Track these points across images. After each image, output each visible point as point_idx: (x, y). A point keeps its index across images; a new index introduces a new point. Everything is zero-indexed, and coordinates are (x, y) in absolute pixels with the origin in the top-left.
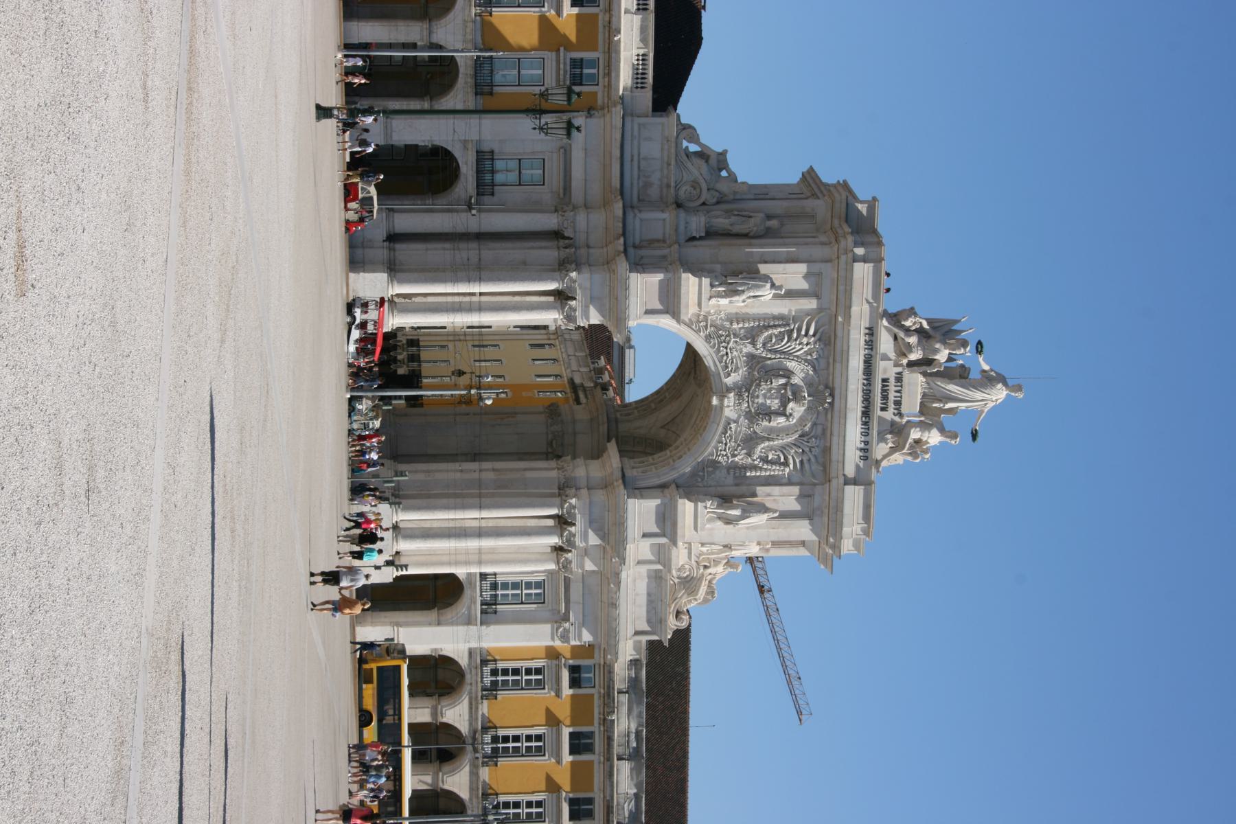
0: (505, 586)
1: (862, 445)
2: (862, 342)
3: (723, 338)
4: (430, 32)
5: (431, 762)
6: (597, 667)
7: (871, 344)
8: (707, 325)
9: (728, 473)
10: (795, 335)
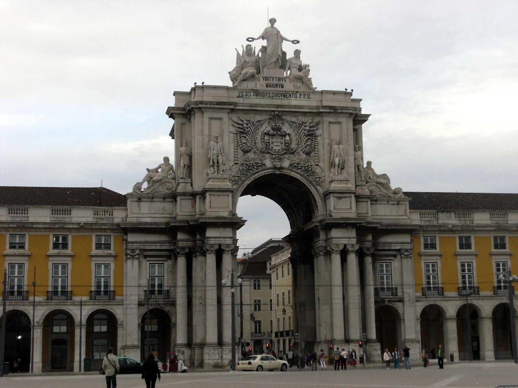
1: (302, 97)
2: (247, 97)
5: (478, 322)
6: (424, 235)
8: (237, 176)
9: (317, 165)
10: (242, 131)
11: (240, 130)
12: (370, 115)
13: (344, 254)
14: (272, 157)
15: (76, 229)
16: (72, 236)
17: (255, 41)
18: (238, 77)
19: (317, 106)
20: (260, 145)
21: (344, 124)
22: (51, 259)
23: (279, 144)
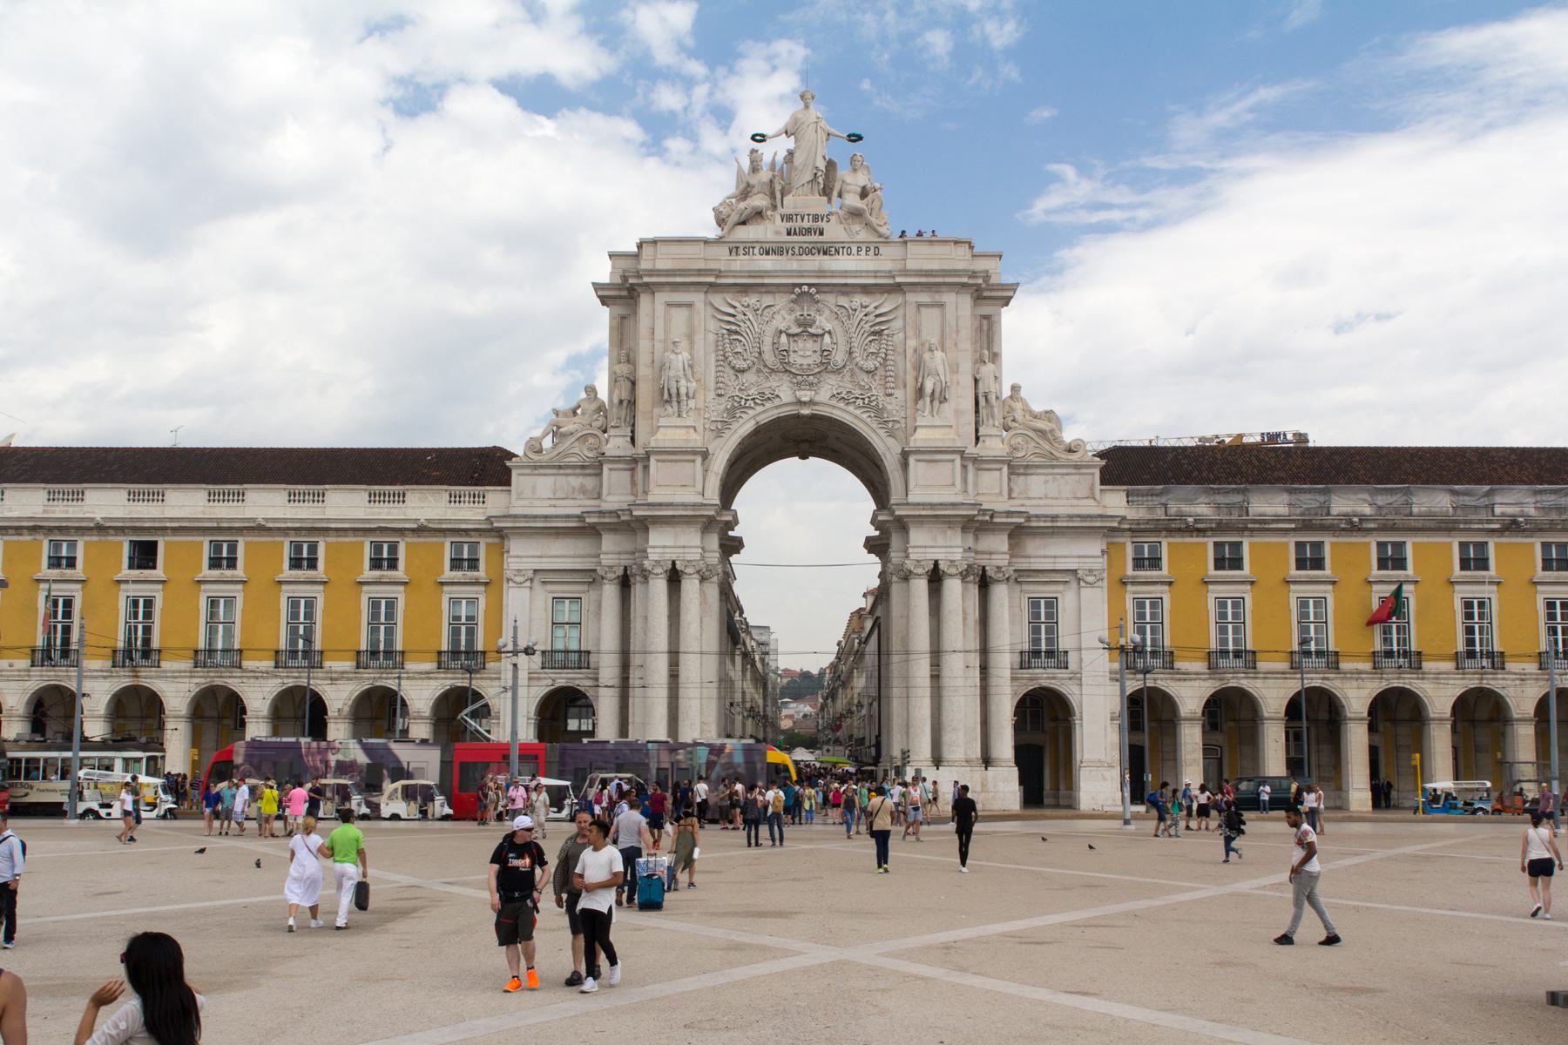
0: (1036, 641)
2: (747, 257)
3: (736, 404)
4: (422, 718)
6: (1135, 540)
7: (748, 248)
9: (891, 395)
10: (734, 328)
11: (728, 327)
12: (1018, 284)
13: (936, 578)
14: (795, 381)
15: (413, 530)
16: (407, 543)
17: (768, 140)
18: (729, 216)
19: (890, 271)
20: (769, 358)
21: (950, 309)
22: (365, 588)
23: (808, 353)
